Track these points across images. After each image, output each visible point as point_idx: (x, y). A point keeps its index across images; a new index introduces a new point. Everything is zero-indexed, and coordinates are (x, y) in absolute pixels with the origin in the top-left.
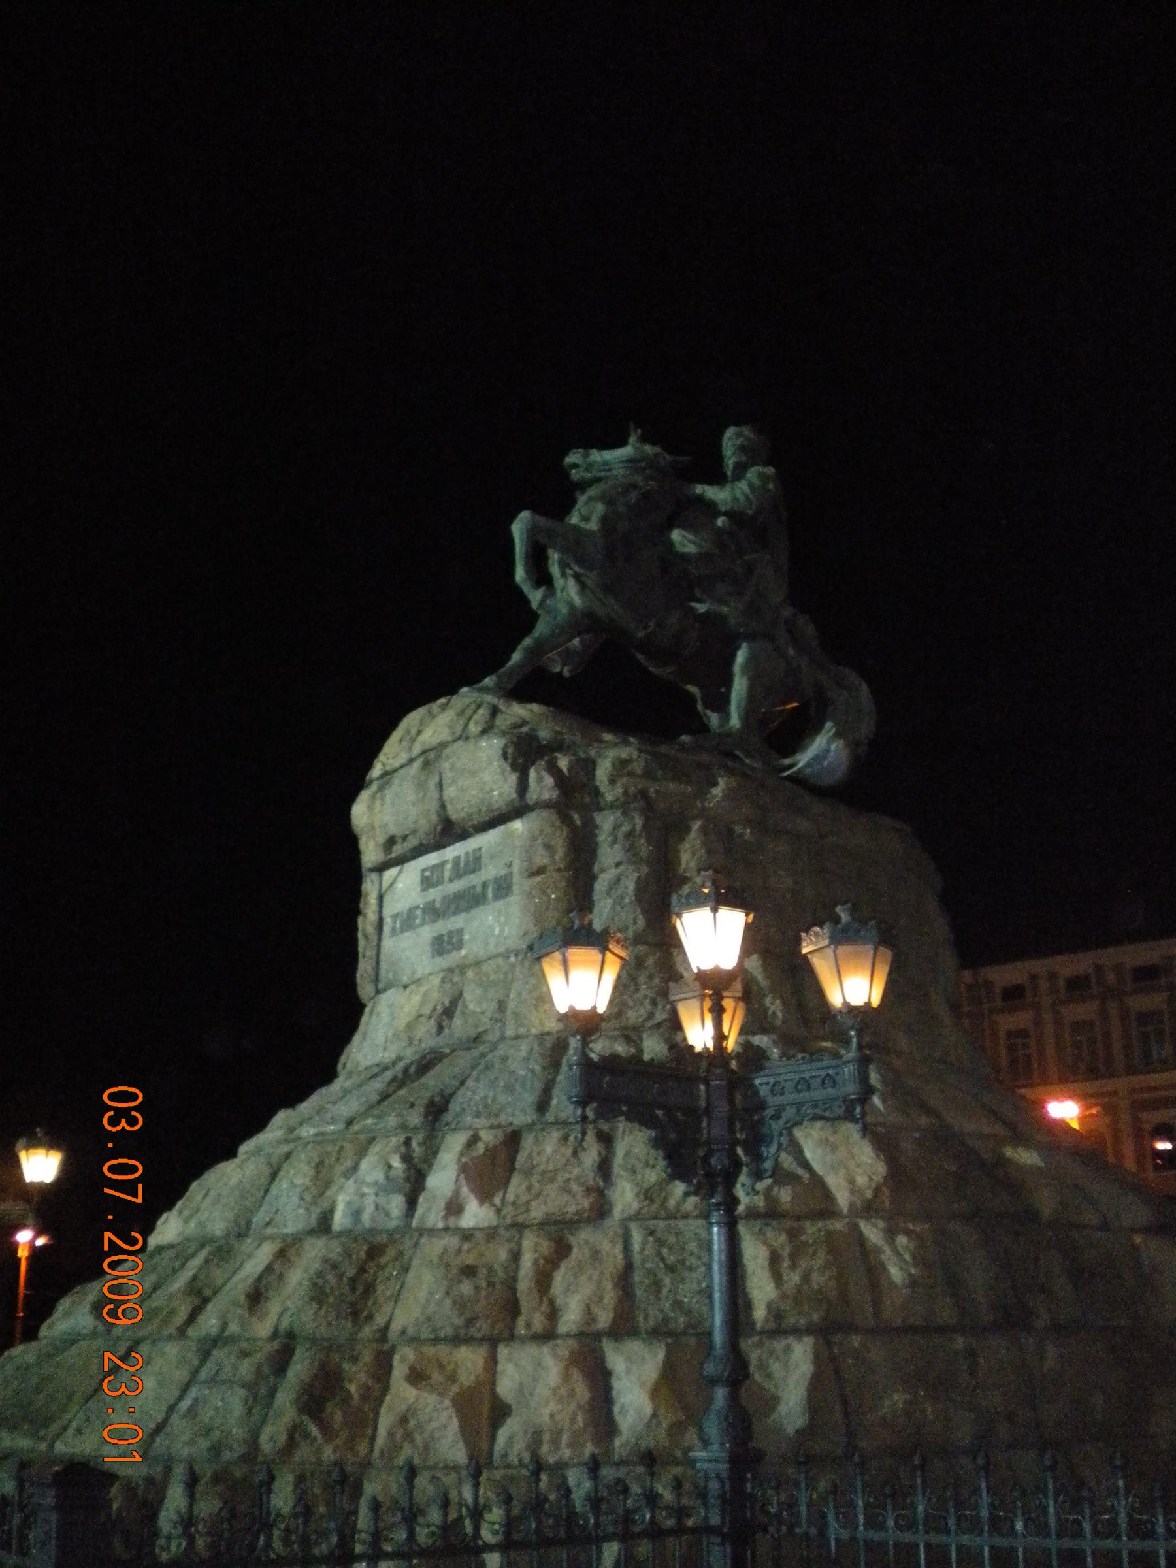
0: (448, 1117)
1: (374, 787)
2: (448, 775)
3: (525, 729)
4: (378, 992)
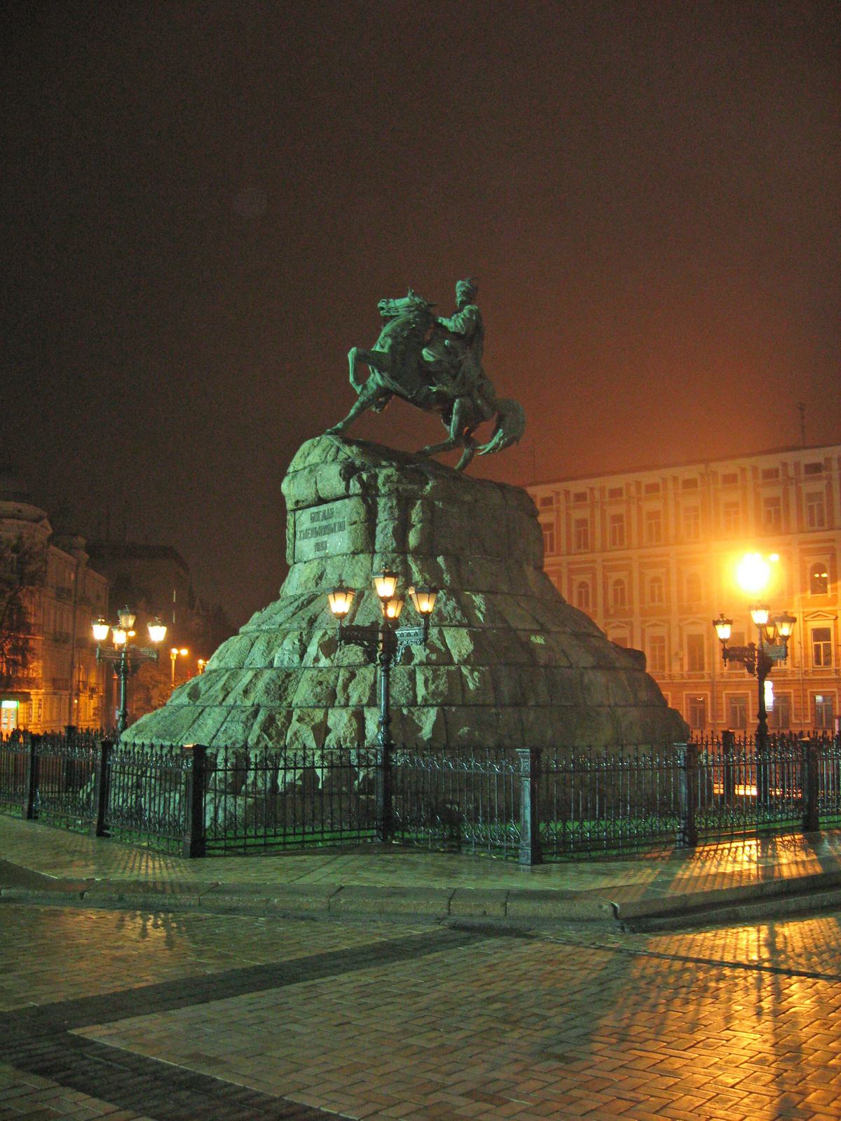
0: (316, 624)
1: (290, 476)
2: (318, 478)
3: (350, 460)
4: (295, 563)
